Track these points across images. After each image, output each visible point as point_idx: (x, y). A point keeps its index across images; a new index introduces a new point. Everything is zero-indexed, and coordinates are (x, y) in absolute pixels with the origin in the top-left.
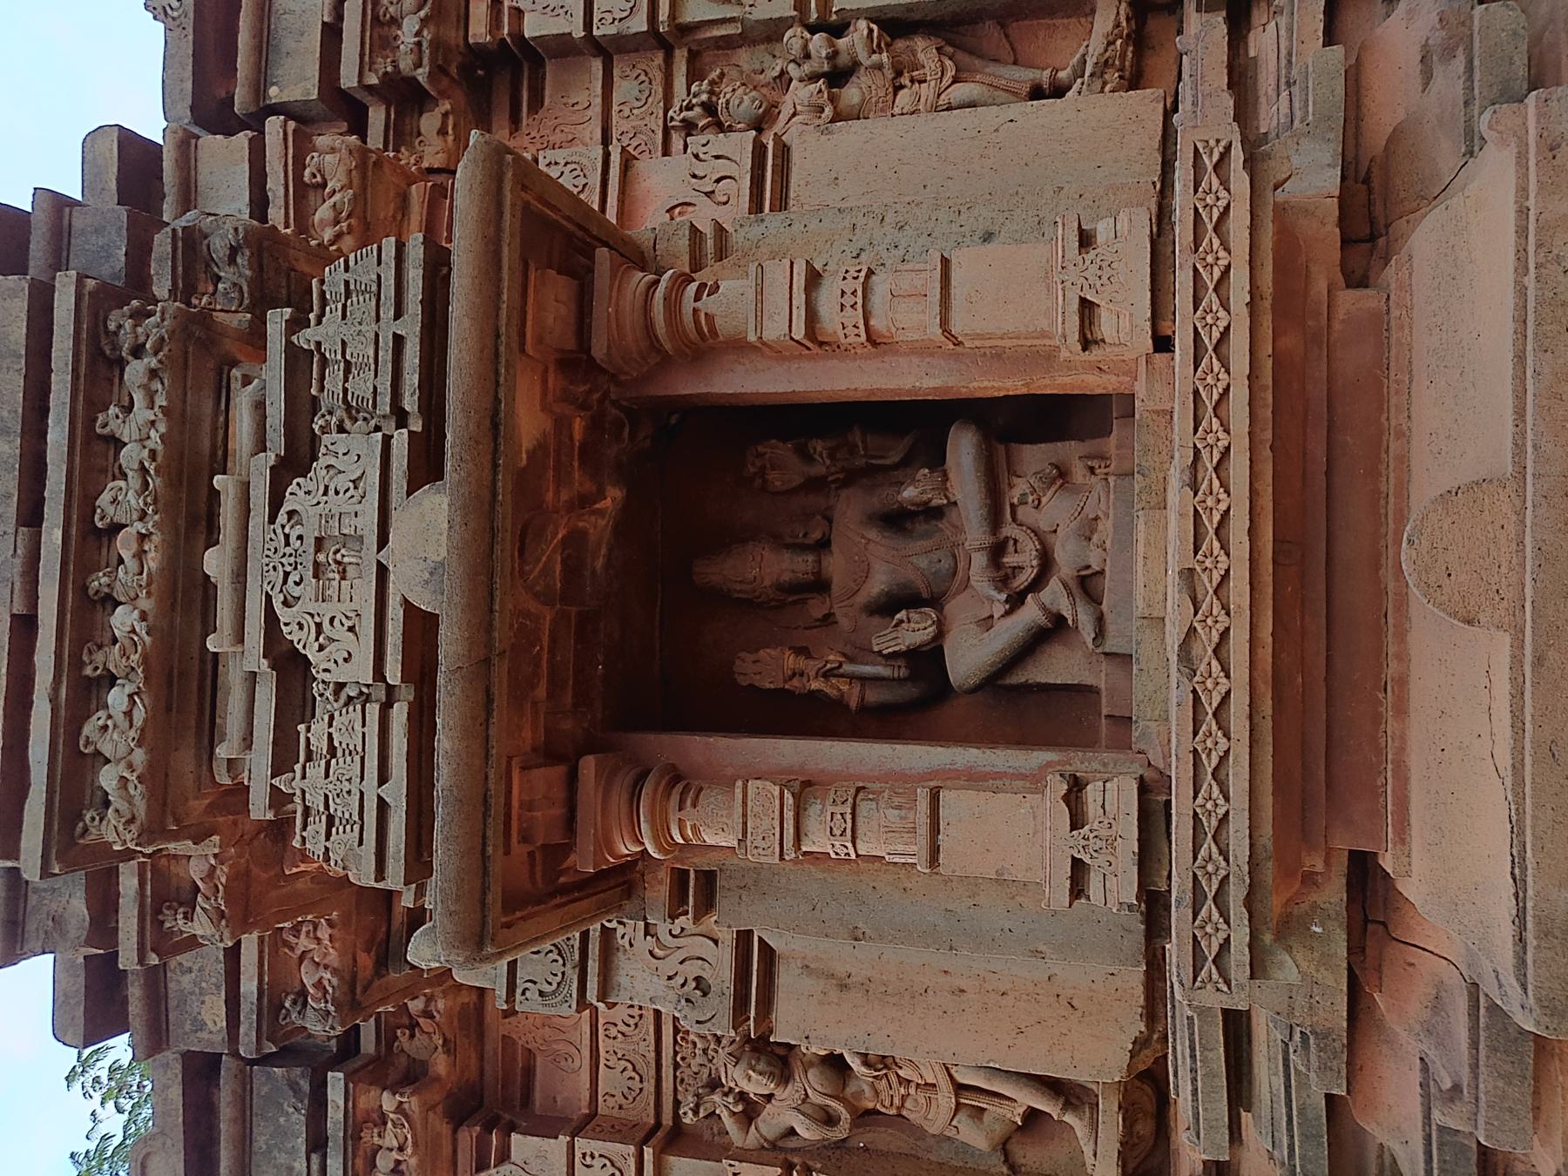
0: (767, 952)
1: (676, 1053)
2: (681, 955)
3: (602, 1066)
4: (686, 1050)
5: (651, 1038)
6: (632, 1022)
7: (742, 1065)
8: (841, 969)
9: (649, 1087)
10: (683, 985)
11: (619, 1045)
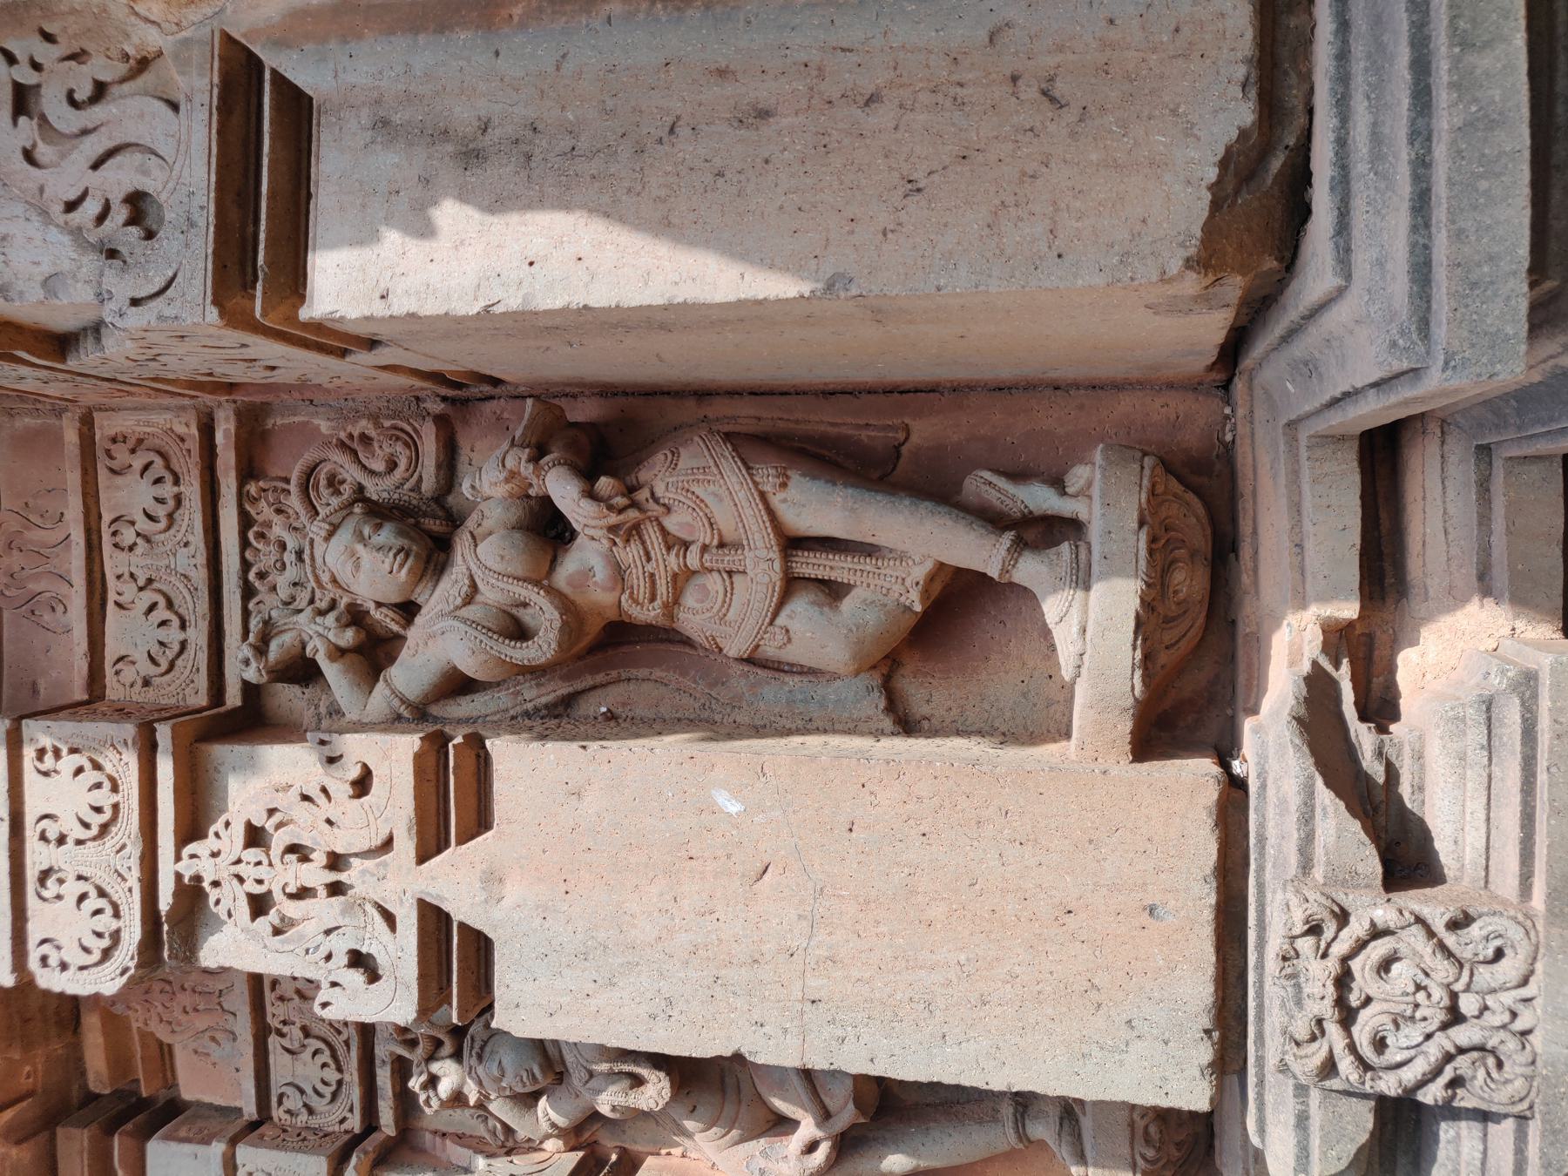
0: (298, 109)
1: (246, 565)
2: (94, 146)
3: (110, 606)
4: (265, 557)
5: (198, 539)
6: (161, 512)
7: (344, 536)
8: (463, 115)
9: (198, 636)
10: (101, 219)
11: (140, 563)
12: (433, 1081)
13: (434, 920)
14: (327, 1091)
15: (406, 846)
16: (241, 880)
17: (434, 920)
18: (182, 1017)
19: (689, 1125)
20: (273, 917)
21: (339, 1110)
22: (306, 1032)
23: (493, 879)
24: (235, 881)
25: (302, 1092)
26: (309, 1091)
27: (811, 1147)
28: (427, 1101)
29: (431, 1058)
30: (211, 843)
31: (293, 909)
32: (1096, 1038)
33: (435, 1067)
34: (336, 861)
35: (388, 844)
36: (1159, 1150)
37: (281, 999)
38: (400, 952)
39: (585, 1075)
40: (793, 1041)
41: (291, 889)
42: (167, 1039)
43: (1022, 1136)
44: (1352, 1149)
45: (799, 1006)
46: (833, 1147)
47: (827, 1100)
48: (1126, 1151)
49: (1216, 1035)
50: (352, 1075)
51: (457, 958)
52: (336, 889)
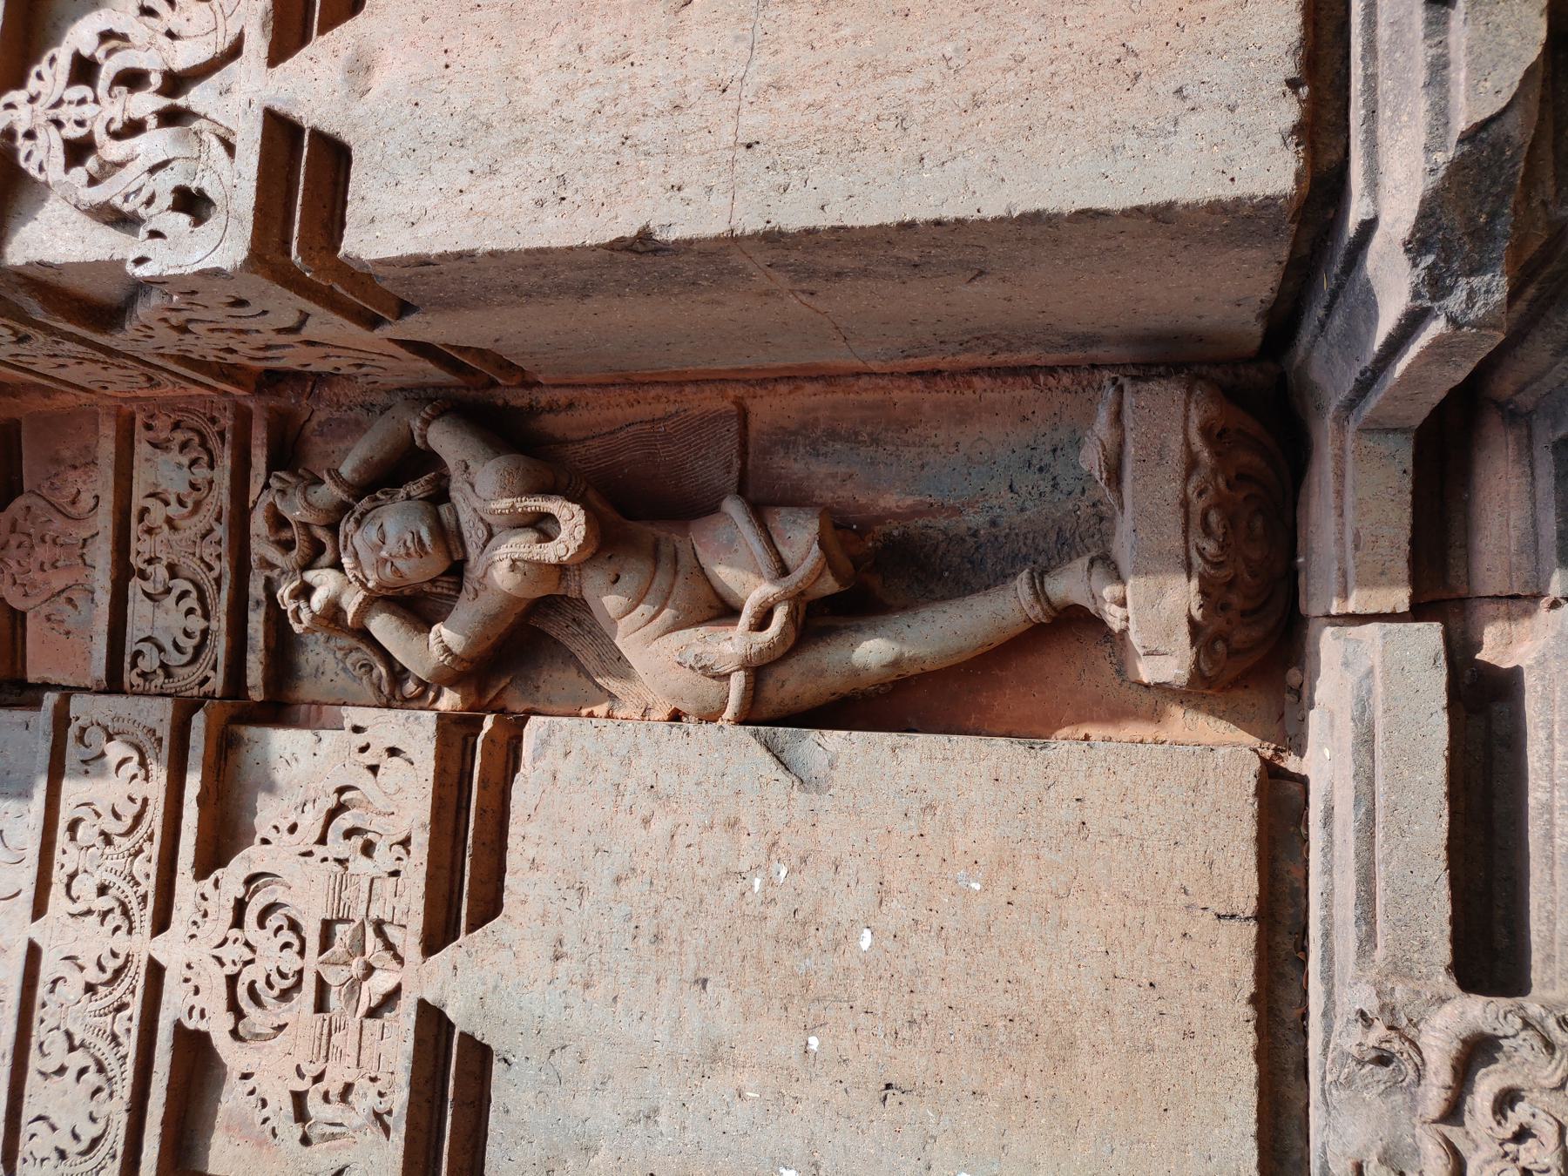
12: (306, 591)
13: (281, 131)
14: (189, 645)
15: (257, 45)
16: (58, 124)
17: (281, 131)
18: (36, 575)
19: (612, 602)
20: (92, 163)
21: (198, 671)
22: (173, 571)
23: (360, 68)
24: (53, 128)
25: (161, 649)
26: (169, 647)
27: (762, 623)
28: (297, 611)
29: (308, 565)
30: (33, 85)
31: (113, 150)
32: (1132, 121)
33: (310, 576)
34: (176, 83)
35: (235, 51)
36: (1221, 548)
37: (150, 531)
38: (235, 182)
39: (482, 532)
40: (719, 201)
41: (116, 126)
42: (18, 603)
43: (1039, 594)
44: (1518, 73)
45: (729, 155)
46: (791, 616)
47: (785, 552)
48: (1178, 543)
49: (1304, 91)
50: (220, 623)
51: (305, 170)
52: (170, 117)
